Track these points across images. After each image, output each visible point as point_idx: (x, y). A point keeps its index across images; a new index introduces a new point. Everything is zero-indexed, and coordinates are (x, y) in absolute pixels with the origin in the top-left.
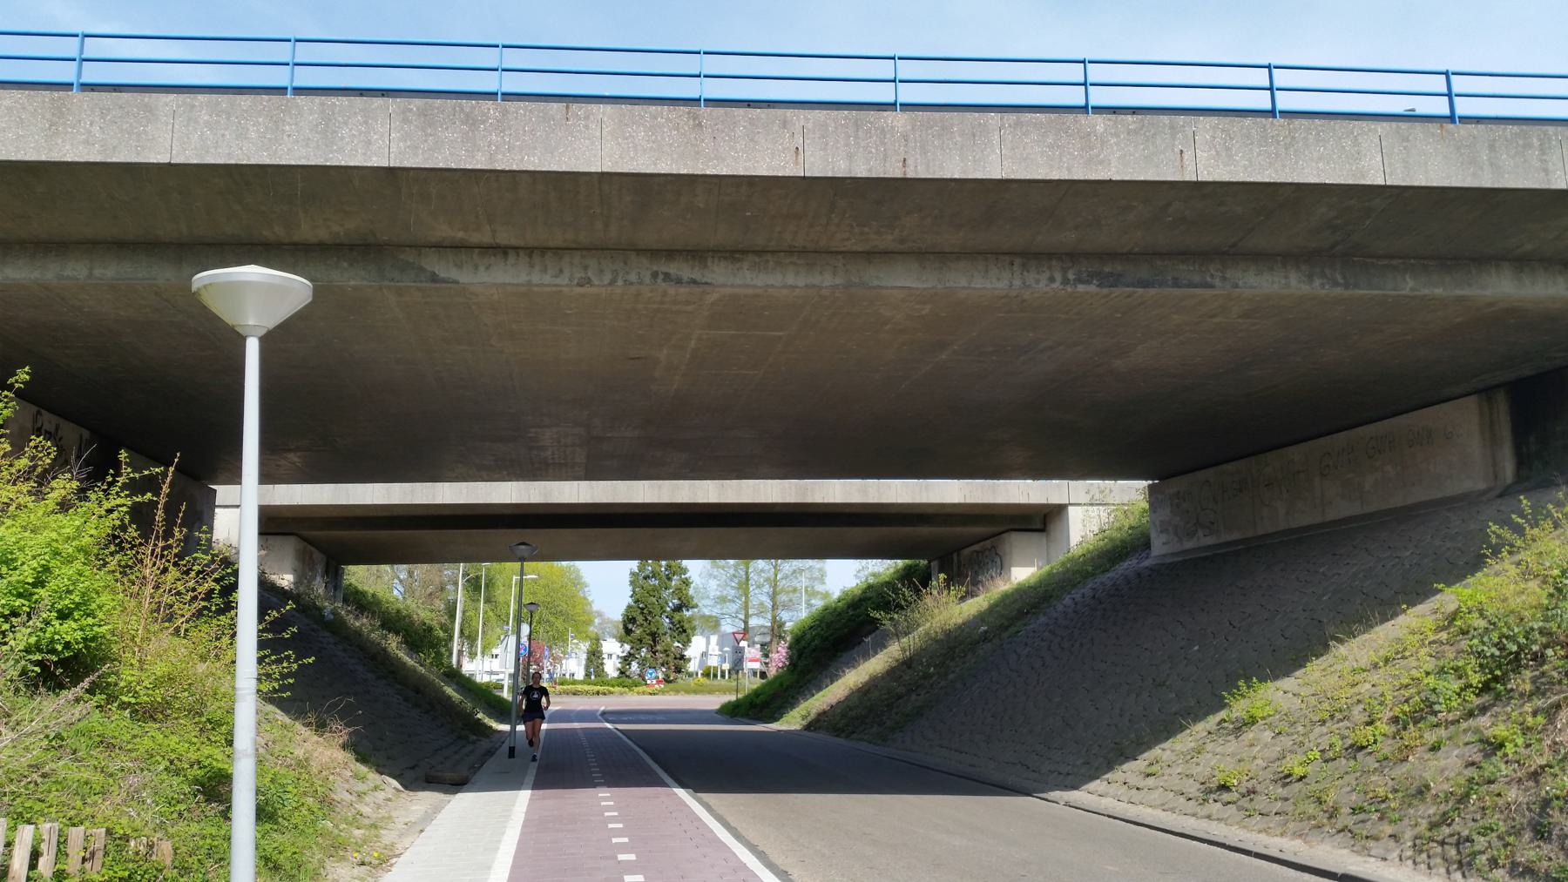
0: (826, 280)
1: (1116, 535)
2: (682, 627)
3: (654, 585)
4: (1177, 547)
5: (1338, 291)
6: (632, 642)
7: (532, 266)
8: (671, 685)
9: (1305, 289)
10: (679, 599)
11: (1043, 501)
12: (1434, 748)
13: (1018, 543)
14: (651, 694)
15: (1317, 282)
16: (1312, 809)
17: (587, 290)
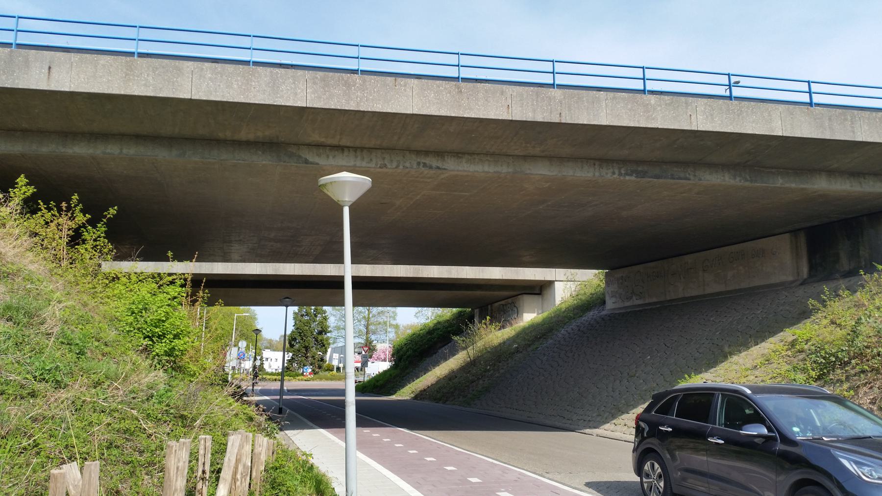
0: (504, 169)
1: (583, 298)
2: (323, 343)
3: (307, 320)
4: (620, 305)
5: (747, 184)
6: (294, 351)
7: (356, 157)
8: (316, 375)
9: (732, 182)
10: (322, 327)
11: (543, 279)
14: (306, 380)
15: (738, 179)
17: (384, 170)
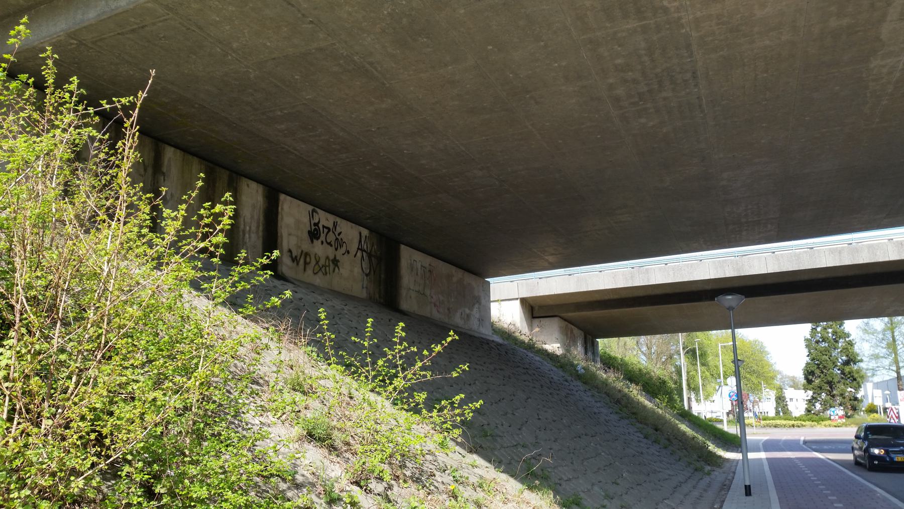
2: (853, 376)
3: (825, 347)
6: (813, 389)
8: (851, 420)
10: (847, 356)
14: (835, 426)
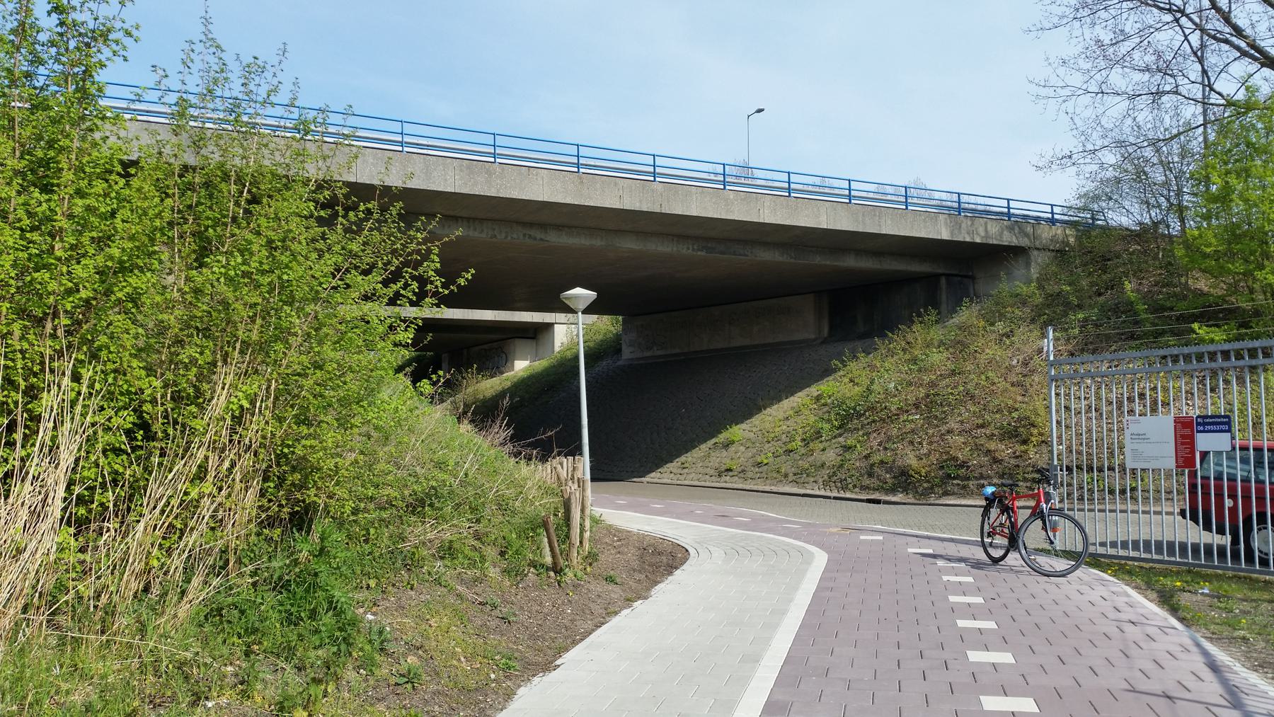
0: (598, 242)
5: (793, 261)
7: (469, 227)
9: (781, 259)
11: (541, 321)
12: (823, 450)
13: (520, 345)
15: (785, 256)
16: (775, 475)
17: (494, 240)
